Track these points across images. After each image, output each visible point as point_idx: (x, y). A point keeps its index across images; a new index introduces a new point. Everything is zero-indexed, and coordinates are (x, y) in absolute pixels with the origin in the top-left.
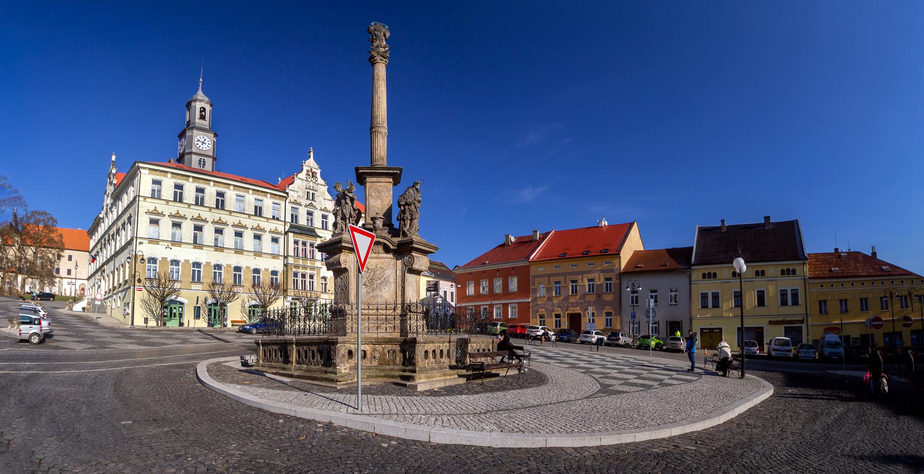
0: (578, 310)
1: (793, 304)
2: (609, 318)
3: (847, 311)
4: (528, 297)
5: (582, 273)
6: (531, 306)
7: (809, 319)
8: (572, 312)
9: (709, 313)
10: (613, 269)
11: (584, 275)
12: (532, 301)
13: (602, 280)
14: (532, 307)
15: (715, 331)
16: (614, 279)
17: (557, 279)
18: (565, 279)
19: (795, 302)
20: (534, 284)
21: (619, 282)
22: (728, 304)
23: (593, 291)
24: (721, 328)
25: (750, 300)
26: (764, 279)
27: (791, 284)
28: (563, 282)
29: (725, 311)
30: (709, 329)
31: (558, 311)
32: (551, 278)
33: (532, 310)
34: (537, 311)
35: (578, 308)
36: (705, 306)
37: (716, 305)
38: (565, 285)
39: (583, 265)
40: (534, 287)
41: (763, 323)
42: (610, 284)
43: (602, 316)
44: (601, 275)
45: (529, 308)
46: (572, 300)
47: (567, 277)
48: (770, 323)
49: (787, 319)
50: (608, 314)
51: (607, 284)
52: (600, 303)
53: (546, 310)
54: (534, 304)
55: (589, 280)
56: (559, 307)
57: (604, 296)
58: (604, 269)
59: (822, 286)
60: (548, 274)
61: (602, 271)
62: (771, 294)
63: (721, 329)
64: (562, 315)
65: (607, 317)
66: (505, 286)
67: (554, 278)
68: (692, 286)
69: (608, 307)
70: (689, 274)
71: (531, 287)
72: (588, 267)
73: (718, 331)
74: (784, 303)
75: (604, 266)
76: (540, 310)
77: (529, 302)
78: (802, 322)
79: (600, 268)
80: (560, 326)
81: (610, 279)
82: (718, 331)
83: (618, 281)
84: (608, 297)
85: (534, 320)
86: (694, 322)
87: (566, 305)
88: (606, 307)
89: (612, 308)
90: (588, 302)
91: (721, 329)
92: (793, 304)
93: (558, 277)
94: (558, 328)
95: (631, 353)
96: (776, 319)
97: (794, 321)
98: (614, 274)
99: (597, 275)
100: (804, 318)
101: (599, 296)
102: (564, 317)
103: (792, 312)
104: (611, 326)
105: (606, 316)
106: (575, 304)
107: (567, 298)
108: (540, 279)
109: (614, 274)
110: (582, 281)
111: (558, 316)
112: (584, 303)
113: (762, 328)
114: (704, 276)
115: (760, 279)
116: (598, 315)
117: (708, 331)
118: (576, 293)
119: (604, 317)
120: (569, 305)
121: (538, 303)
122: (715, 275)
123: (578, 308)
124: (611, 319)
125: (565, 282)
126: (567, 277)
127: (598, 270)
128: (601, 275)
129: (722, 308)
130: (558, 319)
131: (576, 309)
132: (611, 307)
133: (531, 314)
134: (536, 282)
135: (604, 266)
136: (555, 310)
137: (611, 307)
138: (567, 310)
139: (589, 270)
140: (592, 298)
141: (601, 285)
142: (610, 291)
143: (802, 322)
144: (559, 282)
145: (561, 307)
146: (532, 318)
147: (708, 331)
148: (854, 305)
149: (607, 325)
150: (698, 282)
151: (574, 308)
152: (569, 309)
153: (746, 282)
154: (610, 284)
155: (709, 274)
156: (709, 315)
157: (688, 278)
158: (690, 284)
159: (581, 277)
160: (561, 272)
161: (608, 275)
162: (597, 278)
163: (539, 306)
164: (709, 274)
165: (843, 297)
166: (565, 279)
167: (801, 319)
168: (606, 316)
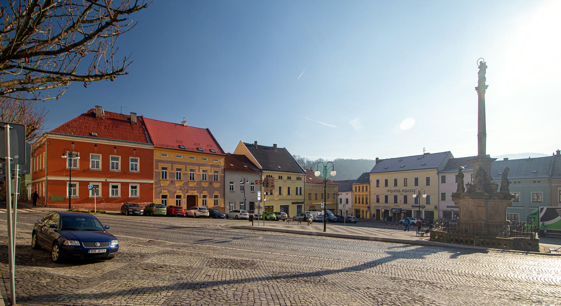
0: (195, 193)
1: (271, 194)
2: (216, 199)
4: (151, 178)
5: (199, 165)
6: (154, 187)
8: (191, 194)
10: (219, 165)
11: (201, 167)
12: (156, 183)
14: (155, 188)
15: (270, 207)
16: (220, 172)
17: (179, 166)
18: (186, 167)
21: (223, 175)
23: (206, 180)
24: (280, 206)
26: (290, 181)
27: (300, 184)
31: (179, 193)
32: (174, 165)
33: (156, 191)
35: (196, 191)
38: (186, 173)
39: (197, 159)
40: (157, 170)
43: (212, 198)
45: (152, 189)
46: (191, 185)
47: (188, 166)
48: (293, 203)
49: (298, 201)
50: (216, 197)
52: (211, 189)
53: (169, 191)
55: (203, 171)
56: (180, 189)
57: (214, 184)
61: (212, 166)
63: (273, 206)
64: (183, 196)
66: (125, 164)
67: (162, 164)
70: (261, 175)
71: (155, 170)
72: (204, 162)
76: (163, 191)
77: (152, 184)
78: (303, 203)
80: (217, 205)
82: (272, 207)
83: (223, 175)
84: (216, 185)
88: (204, 192)
90: (203, 187)
91: (273, 206)
92: (271, 194)
94: (216, 206)
95: (269, 223)
98: (221, 169)
99: (209, 168)
101: (211, 183)
102: (184, 198)
103: (300, 198)
105: (162, 198)
106: (194, 189)
107: (186, 184)
109: (221, 169)
110: (199, 171)
111: (179, 197)
112: (200, 188)
116: (170, 197)
117: (267, 207)
118: (193, 179)
120: (189, 189)
121: (162, 185)
126: (188, 166)
127: (210, 165)
129: (274, 195)
130: (178, 199)
131: (194, 191)
132: (218, 192)
133: (154, 195)
134: (159, 166)
136: (177, 191)
137: (218, 192)
138: (187, 192)
139: (205, 163)
140: (205, 185)
143: (303, 203)
144: (180, 170)
145: (182, 190)
146: (156, 198)
149: (215, 205)
151: (192, 191)
152: (189, 192)
153: (284, 182)
154: (205, 174)
155: (269, 176)
157: (260, 177)
159: (197, 168)
161: (217, 169)
162: (209, 170)
163: (162, 188)
166: (186, 167)
167: (302, 201)
168: (162, 198)
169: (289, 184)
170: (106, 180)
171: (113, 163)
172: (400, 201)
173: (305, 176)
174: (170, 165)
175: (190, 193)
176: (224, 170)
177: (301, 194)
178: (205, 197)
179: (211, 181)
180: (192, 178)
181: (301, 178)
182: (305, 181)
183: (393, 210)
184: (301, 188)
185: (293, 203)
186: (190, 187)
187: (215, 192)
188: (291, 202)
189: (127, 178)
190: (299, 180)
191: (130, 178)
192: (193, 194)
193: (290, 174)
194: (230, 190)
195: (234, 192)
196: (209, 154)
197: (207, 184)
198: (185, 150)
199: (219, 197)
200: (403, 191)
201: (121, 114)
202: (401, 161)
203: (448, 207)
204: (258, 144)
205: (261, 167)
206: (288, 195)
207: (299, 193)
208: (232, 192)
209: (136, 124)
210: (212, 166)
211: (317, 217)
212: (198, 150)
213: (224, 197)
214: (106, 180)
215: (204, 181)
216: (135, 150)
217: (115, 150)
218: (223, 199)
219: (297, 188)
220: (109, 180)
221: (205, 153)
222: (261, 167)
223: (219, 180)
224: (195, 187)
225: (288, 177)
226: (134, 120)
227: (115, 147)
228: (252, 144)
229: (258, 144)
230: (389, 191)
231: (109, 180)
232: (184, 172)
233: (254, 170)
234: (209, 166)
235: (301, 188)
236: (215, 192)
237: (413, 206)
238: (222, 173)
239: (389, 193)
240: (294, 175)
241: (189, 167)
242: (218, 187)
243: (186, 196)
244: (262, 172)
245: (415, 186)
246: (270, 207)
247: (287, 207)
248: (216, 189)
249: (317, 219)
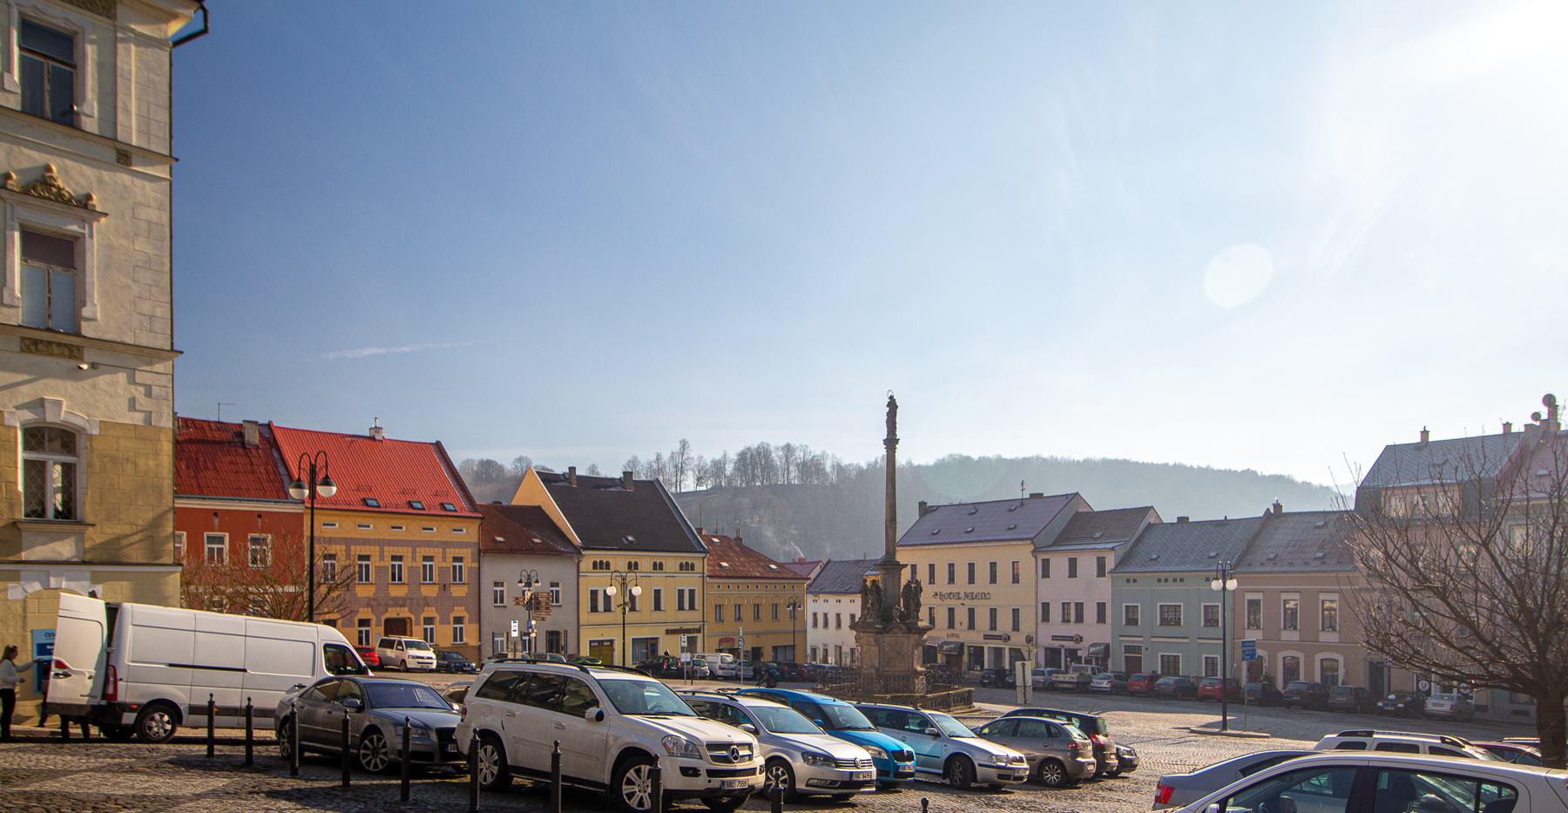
15: (605, 644)
24: (633, 639)
27: (690, 582)
30: (599, 642)
31: (364, 613)
35: (406, 609)
36: (594, 609)
41: (658, 632)
43: (449, 623)
47: (386, 548)
48: (669, 632)
50: (458, 620)
56: (368, 605)
57: (453, 589)
60: (346, 539)
68: (581, 579)
69: (460, 608)
70: (577, 561)
73: (609, 643)
78: (698, 631)
82: (609, 643)
83: (475, 565)
84: (458, 591)
88: (426, 609)
93: (368, 547)
96: (673, 628)
97: (690, 629)
103: (690, 618)
104: (461, 639)
106: (401, 602)
113: (657, 639)
114: (595, 566)
115: (658, 575)
117: (597, 644)
123: (406, 609)
124: (461, 629)
125: (382, 557)
126: (386, 548)
132: (463, 608)
137: (463, 608)
142: (430, 580)
143: (698, 631)
149: (455, 640)
152: (390, 609)
157: (575, 566)
158: (578, 576)
160: (372, 537)
167: (697, 627)
169: (658, 581)
171: (211, 550)
172: (961, 623)
173: (706, 560)
174: (344, 547)
176: (480, 554)
177: (692, 607)
178: (429, 621)
179: (444, 582)
180: (396, 576)
181: (693, 566)
182: (706, 571)
183: (945, 647)
184: (692, 592)
185: (669, 632)
187: (455, 608)
188: (663, 629)
190: (687, 569)
193: (659, 557)
194: (496, 602)
195: (505, 607)
196: (439, 516)
197: (436, 588)
198: (379, 511)
199: (466, 620)
200: (966, 595)
201: (219, 422)
202: (975, 513)
203: (1055, 638)
204: (577, 474)
205: (577, 540)
206: (656, 609)
207: (686, 606)
208: (499, 609)
209: (257, 447)
211: (721, 668)
212: (412, 507)
213: (480, 621)
215: (428, 582)
216: (260, 516)
217: (216, 521)
218: (476, 626)
219: (681, 592)
221: (430, 515)
222: (577, 540)
223: (465, 579)
224: (404, 599)
225: (655, 564)
226: (253, 437)
227: (216, 513)
228: (564, 475)
229: (577, 474)
230: (936, 594)
232: (377, 564)
233: (562, 552)
235: (692, 592)
236: (455, 608)
237: (986, 637)
238: (472, 561)
239: (938, 601)
241: (390, 551)
242: (464, 595)
244: (581, 554)
245: (1013, 583)
246: (605, 644)
247: (653, 641)
248: (458, 601)
249: (720, 672)
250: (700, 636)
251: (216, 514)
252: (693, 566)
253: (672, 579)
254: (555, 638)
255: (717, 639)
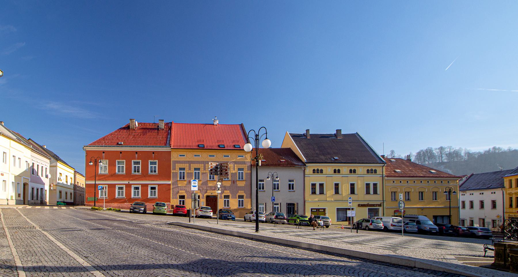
3: (408, 199)
4: (169, 179)
6: (171, 188)
7: (385, 203)
9: (317, 197)
10: (245, 162)
12: (173, 184)
13: (236, 170)
14: (172, 189)
19: (375, 192)
20: (174, 169)
21: (250, 172)
22: (329, 191)
25: (345, 190)
27: (372, 179)
28: (203, 169)
29: (328, 197)
32: (192, 165)
33: (173, 191)
34: (178, 192)
36: (314, 192)
37: (322, 192)
38: (205, 172)
40: (174, 171)
42: (242, 173)
43: (236, 198)
44: (236, 165)
48: (359, 205)
49: (370, 203)
50: (241, 197)
51: (239, 173)
53: (186, 192)
54: (175, 186)
57: (238, 183)
58: (238, 161)
59: (394, 182)
61: (235, 163)
62: (359, 186)
65: (240, 199)
68: (306, 178)
70: (303, 169)
71: (172, 171)
74: (368, 192)
75: (238, 159)
76: (180, 191)
77: (170, 185)
79: (234, 160)
81: (242, 169)
85: (175, 200)
86: (306, 204)
87: (205, 188)
89: (244, 192)
98: (246, 165)
100: (381, 203)
103: (373, 199)
106: (213, 188)
107: (205, 183)
108: (181, 165)
109: (246, 165)
117: (316, 210)
119: (238, 199)
121: (179, 185)
122: (322, 171)
124: (242, 201)
127: (233, 162)
128: (236, 165)
129: (326, 194)
132: (243, 191)
134: (176, 167)
135: (238, 159)
138: (206, 192)
141: (236, 173)
146: (173, 198)
147: (316, 210)
148: (414, 196)
149: (239, 206)
150: (310, 176)
151: (212, 191)
152: (208, 191)
156: (317, 200)
158: (304, 177)
161: (241, 166)
162: (232, 168)
163: (179, 188)
164: (318, 170)
165: (407, 190)
170: (129, 182)
175: (209, 193)
186: (209, 187)
189: (146, 180)
191: (149, 180)
192: (213, 194)
197: (230, 182)
210: (235, 163)
214: (129, 182)
220: (131, 182)
231: (131, 182)
234: (232, 163)
240: (362, 168)
243: (205, 196)
248: (241, 188)
250: (381, 209)
251: (136, 153)
252: (375, 171)
253: (347, 178)
254: (292, 206)
255: (393, 210)
